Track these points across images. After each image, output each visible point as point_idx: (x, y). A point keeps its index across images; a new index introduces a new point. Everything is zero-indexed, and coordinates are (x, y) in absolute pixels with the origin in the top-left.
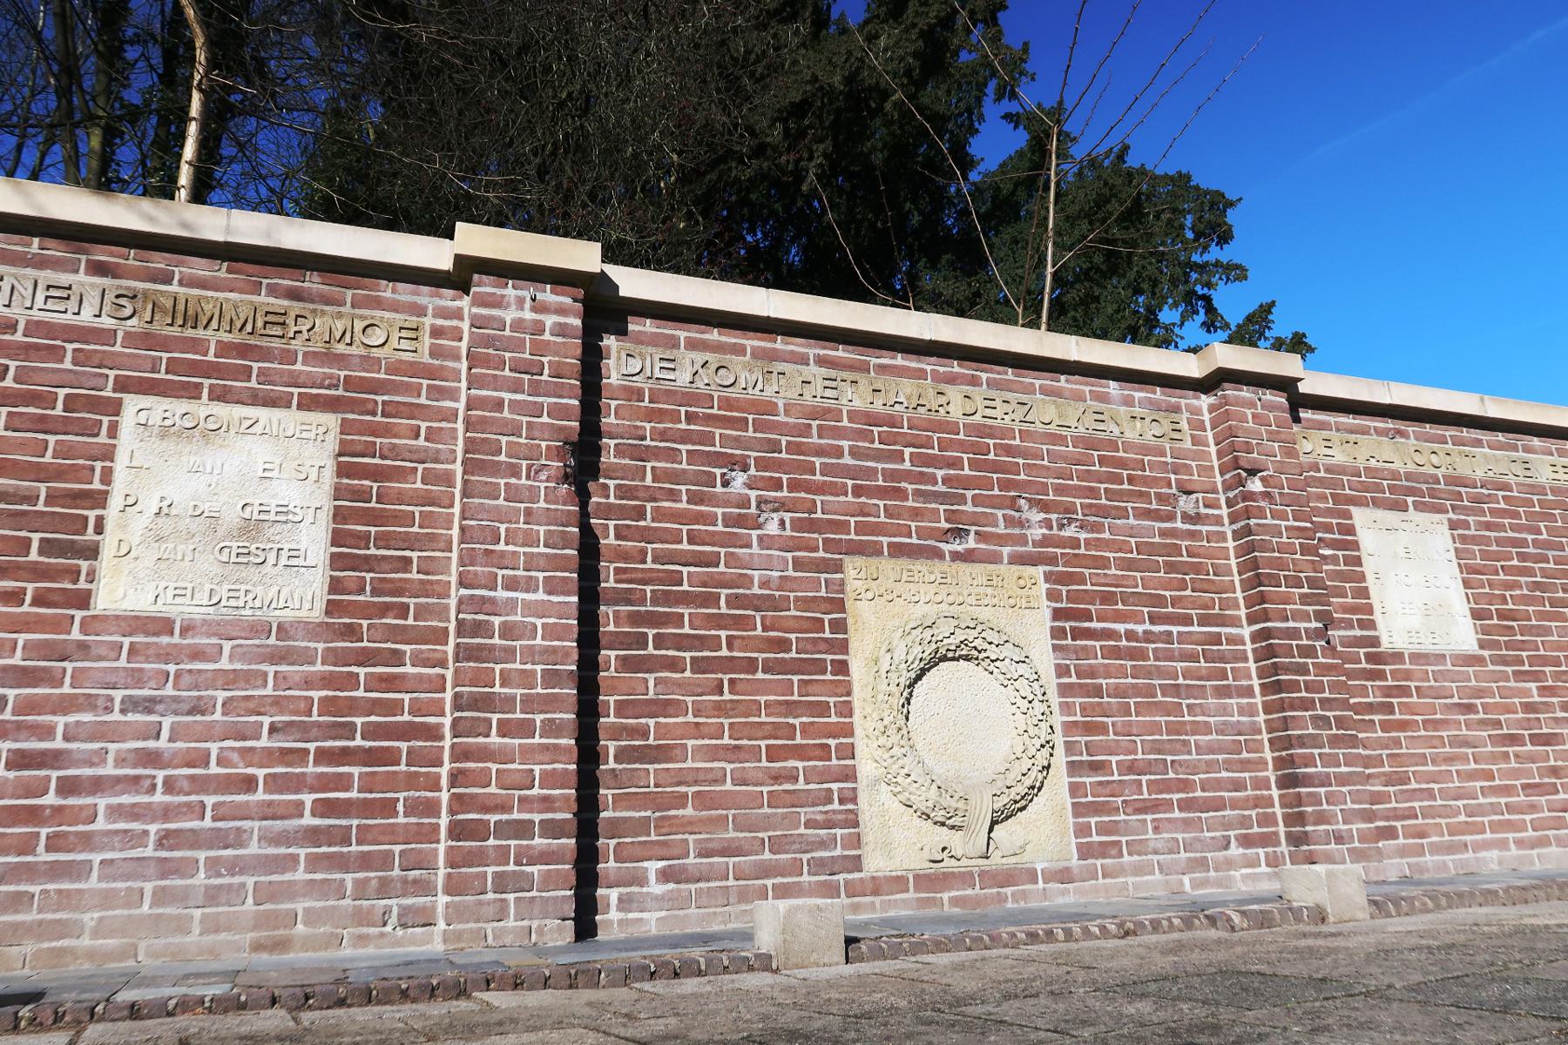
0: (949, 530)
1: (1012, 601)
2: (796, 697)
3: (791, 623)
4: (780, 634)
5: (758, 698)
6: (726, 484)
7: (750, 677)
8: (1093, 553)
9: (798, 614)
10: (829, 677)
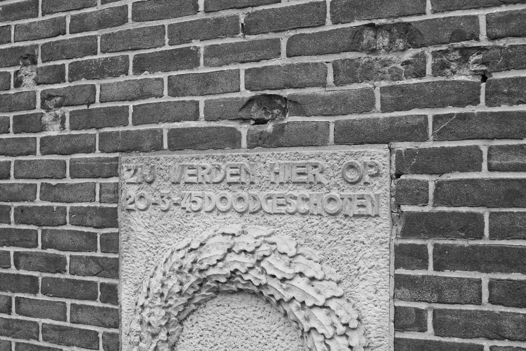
0: (251, 101)
1: (332, 208)
2: (68, 324)
3: (66, 240)
4: (57, 252)
5: (37, 320)
6: (18, 83)
7: (32, 297)
8: (504, 108)
9: (74, 228)
10: (97, 304)
